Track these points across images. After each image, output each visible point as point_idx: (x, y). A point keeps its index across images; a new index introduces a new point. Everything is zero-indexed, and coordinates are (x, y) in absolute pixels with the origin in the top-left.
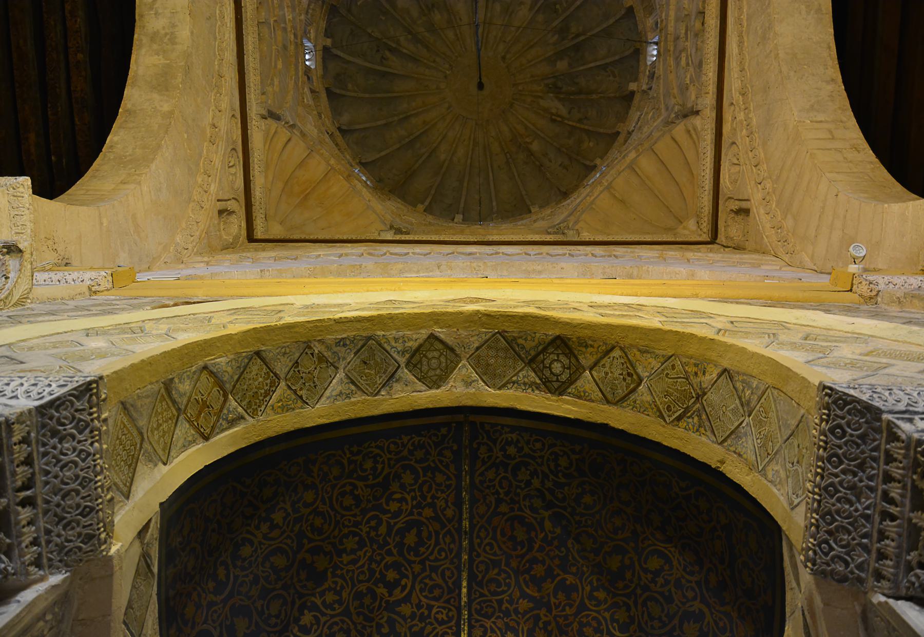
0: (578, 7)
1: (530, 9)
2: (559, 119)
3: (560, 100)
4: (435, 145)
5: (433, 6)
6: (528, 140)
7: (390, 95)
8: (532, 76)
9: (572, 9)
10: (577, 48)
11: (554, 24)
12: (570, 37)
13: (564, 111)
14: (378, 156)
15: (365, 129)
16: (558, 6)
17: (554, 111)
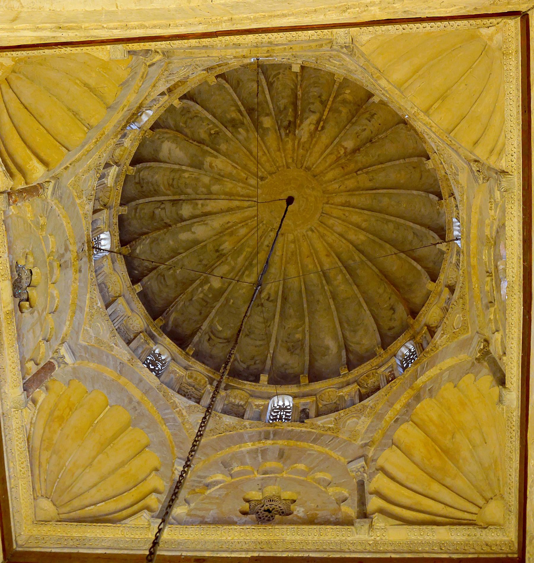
0: (214, 115)
1: (216, 157)
2: (322, 123)
3: (302, 122)
4: (351, 246)
5: (217, 251)
6: (342, 152)
7: (304, 295)
8: (279, 150)
9: (215, 121)
10: (250, 111)
11: (229, 134)
12: (241, 117)
13: (313, 118)
14: (368, 312)
15: (341, 323)
16: (212, 132)
17: (312, 127)
